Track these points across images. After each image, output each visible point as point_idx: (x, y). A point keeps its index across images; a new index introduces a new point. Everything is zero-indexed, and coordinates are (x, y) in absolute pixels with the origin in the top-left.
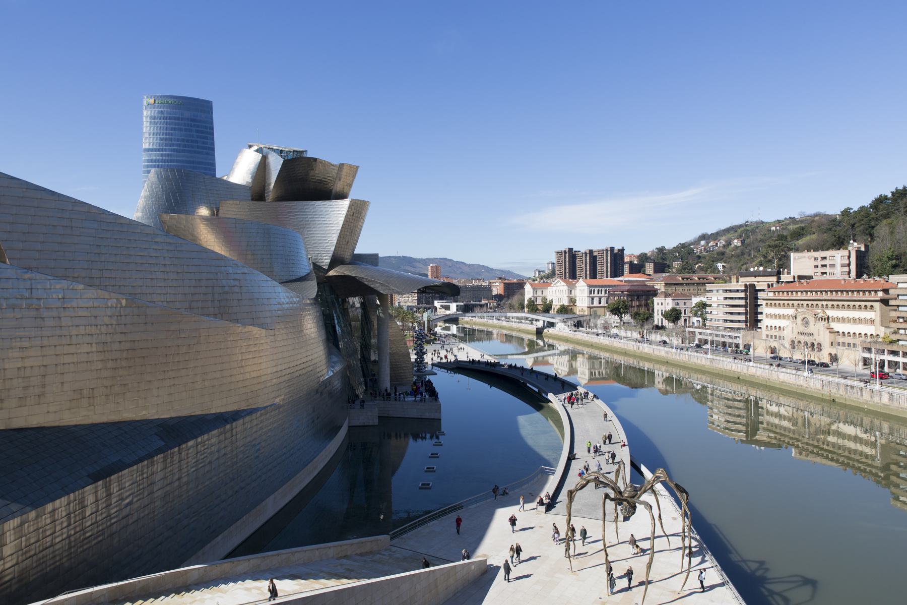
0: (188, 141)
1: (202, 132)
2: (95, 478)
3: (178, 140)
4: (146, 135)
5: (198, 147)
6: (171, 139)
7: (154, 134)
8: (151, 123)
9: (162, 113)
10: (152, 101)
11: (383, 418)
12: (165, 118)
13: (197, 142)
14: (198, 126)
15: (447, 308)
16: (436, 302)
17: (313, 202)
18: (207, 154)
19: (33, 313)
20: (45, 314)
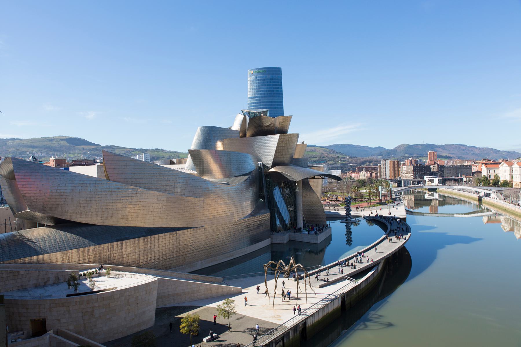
0: (269, 91)
1: (276, 85)
2: (118, 241)
3: (264, 91)
4: (249, 90)
5: (274, 94)
6: (261, 91)
7: (253, 89)
8: (251, 83)
9: (256, 77)
10: (252, 72)
11: (291, 241)
12: (258, 80)
13: (273, 91)
14: (274, 82)
15: (432, 181)
16: (425, 177)
17: (268, 136)
18: (279, 97)
19: (110, 193)
20: (113, 193)
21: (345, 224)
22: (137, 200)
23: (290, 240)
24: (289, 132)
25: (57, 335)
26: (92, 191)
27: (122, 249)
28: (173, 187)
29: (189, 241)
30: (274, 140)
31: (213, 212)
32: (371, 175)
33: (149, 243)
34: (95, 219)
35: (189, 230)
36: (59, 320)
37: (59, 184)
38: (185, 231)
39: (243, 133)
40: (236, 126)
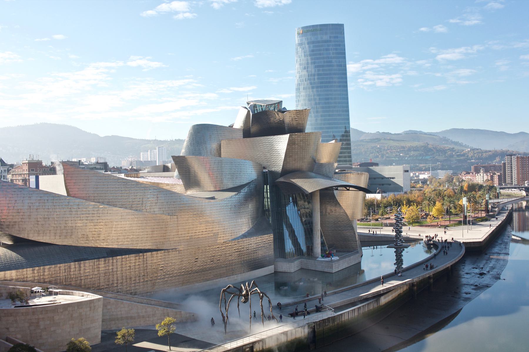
2: (75, 261)
17: (276, 137)
19: (69, 210)
20: (73, 210)
21: (394, 250)
22: (98, 218)
23: (302, 269)
24: (306, 131)
25: (7, 341)
26: (49, 207)
27: (80, 270)
28: (140, 203)
29: (159, 264)
30: (281, 142)
31: (191, 232)
32: (492, 177)
33: (111, 264)
34: (53, 238)
35: (159, 252)
36: (8, 329)
37: (16, 201)
38: (154, 253)
39: (247, 133)
40: (239, 124)
